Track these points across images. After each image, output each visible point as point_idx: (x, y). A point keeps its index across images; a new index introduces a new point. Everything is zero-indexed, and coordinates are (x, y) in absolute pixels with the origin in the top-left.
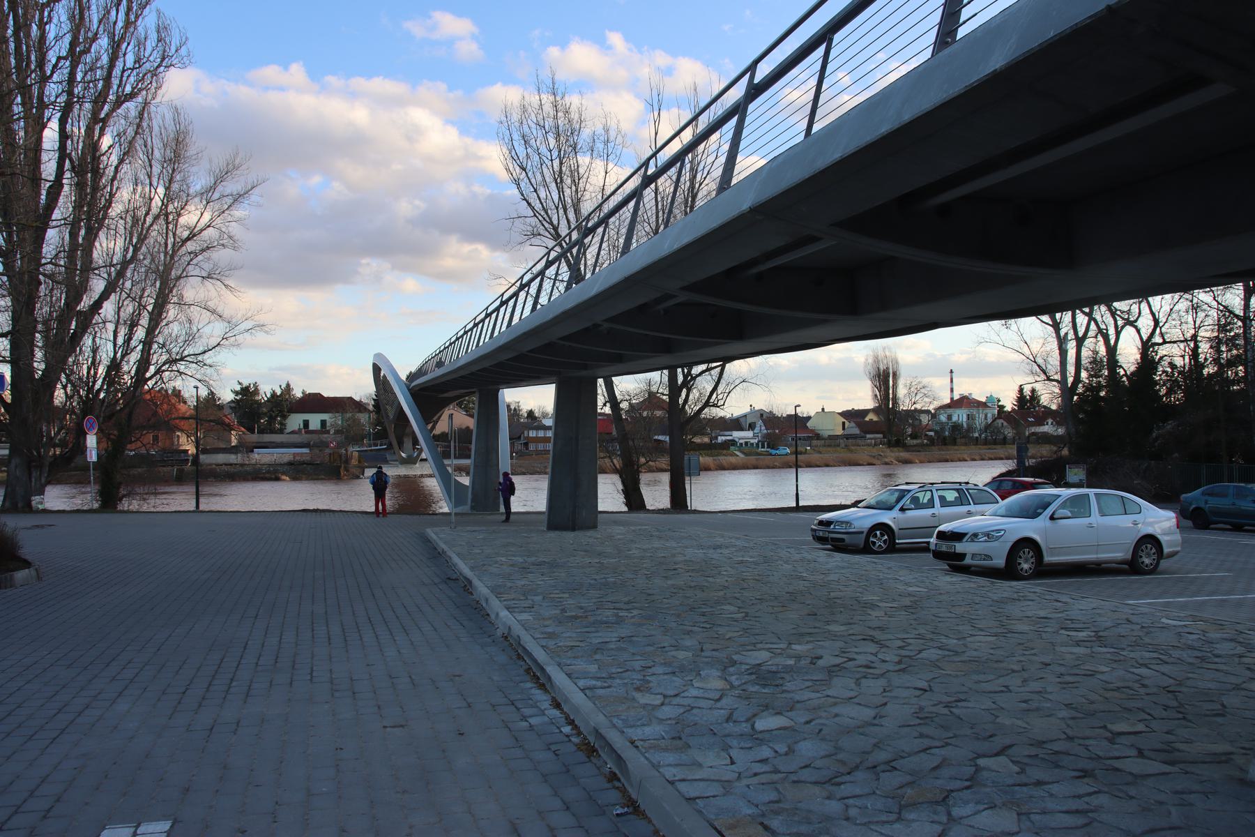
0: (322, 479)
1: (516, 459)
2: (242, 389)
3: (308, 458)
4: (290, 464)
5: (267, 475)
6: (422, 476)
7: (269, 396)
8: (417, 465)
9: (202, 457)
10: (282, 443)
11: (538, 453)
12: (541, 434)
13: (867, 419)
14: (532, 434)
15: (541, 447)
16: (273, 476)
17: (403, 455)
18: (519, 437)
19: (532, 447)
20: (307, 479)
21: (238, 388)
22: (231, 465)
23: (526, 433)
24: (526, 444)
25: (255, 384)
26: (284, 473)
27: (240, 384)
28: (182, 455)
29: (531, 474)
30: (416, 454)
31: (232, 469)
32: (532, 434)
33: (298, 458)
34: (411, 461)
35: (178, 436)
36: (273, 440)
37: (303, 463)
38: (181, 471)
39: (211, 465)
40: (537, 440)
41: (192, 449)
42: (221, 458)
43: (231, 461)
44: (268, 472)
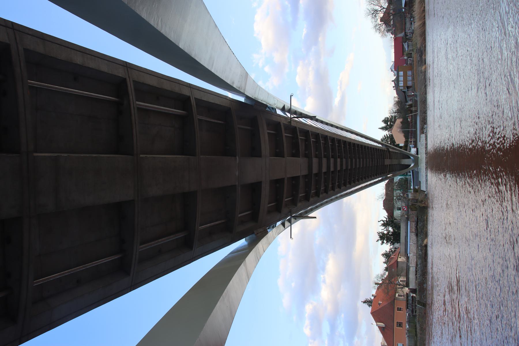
0: (427, 218)
1: (417, 92)
2: (381, 240)
3: (414, 224)
4: (417, 235)
5: (423, 251)
6: (426, 153)
7: (383, 228)
8: (419, 156)
9: (411, 287)
10: (405, 232)
11: (413, 79)
12: (401, 79)
14: (401, 84)
16: (424, 248)
17: (412, 165)
18: (404, 92)
19: (410, 84)
21: (380, 242)
22: (416, 271)
23: (402, 88)
24: (408, 87)
25: (379, 233)
26: (423, 241)
27: (378, 241)
29: (426, 82)
30: (412, 157)
31: (419, 272)
32: (401, 84)
33: (413, 230)
34: (416, 161)
37: (417, 227)
38: (419, 303)
39: (416, 283)
40: (405, 81)
42: (412, 276)
44: (421, 250)
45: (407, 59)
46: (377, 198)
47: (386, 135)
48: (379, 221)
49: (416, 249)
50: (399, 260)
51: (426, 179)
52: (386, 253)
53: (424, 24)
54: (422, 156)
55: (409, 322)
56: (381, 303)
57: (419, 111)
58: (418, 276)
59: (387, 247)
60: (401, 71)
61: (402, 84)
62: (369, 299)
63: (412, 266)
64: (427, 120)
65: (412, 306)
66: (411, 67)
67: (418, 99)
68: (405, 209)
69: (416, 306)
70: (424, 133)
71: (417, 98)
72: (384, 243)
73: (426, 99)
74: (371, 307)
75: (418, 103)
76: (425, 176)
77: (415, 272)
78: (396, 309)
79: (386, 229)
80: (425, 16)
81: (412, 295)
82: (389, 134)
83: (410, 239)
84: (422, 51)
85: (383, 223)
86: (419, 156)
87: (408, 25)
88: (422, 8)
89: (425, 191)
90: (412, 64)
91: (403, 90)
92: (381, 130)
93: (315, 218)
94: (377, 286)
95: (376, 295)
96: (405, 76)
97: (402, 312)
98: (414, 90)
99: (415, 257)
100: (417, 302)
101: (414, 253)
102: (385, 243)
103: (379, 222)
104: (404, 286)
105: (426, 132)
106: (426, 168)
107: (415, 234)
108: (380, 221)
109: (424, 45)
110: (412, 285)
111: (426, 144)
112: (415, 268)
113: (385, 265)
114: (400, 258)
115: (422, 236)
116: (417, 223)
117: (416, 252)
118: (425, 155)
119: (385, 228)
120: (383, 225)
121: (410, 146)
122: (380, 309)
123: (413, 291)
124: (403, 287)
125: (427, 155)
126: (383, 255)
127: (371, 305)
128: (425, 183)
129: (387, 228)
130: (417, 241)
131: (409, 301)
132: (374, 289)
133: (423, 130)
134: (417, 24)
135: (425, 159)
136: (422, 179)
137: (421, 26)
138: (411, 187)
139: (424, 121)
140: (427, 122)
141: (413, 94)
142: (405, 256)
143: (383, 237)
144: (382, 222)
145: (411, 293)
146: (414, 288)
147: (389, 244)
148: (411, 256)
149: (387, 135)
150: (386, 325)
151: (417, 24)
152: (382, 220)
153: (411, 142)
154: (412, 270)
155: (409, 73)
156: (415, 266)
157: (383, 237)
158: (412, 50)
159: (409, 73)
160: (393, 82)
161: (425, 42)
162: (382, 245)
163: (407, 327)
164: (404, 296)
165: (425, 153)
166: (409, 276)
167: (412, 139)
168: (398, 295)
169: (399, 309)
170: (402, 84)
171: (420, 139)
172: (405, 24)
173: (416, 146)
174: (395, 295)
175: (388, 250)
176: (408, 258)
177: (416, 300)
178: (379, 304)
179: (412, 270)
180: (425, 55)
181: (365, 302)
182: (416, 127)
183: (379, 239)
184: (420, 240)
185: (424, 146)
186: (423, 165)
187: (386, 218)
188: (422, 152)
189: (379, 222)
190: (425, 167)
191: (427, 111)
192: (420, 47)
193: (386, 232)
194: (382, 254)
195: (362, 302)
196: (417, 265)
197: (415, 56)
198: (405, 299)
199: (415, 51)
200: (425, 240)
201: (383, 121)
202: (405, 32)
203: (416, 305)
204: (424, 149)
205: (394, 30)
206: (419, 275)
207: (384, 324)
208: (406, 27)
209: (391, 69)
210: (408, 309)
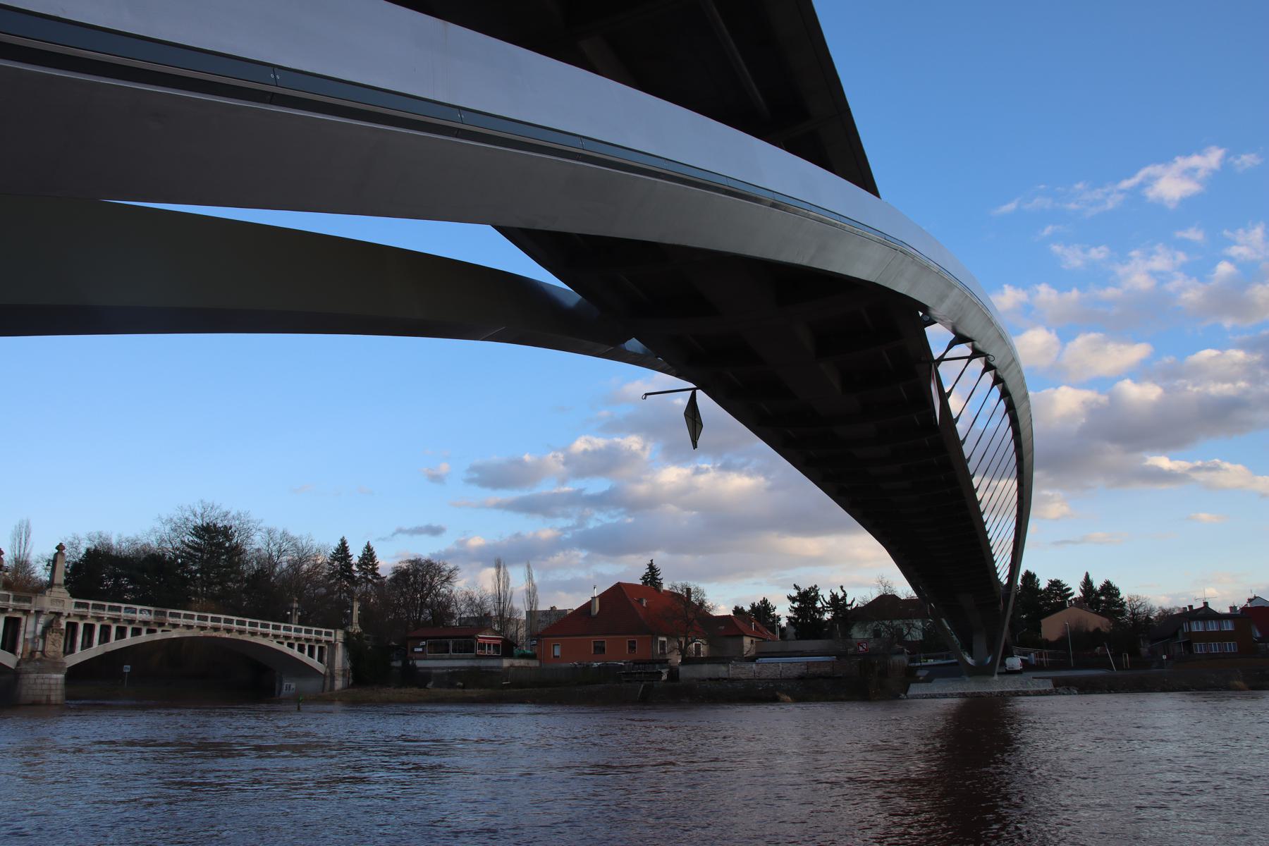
0: (842, 700)
3: (828, 669)
4: (801, 678)
7: (828, 599)
8: (996, 677)
12: (1213, 627)
14: (1197, 627)
17: (969, 660)
18: (1175, 635)
19: (1199, 648)
21: (794, 593)
22: (718, 679)
23: (1185, 626)
24: (1188, 645)
25: (814, 589)
26: (788, 692)
27: (796, 587)
28: (657, 666)
30: (989, 660)
33: (813, 670)
34: (982, 671)
40: (1206, 637)
41: (676, 659)
42: (706, 670)
43: (721, 675)
46: (885, 581)
47: (1070, 592)
48: (844, 589)
49: (769, 677)
50: (747, 641)
51: (938, 696)
52: (770, 609)
54: (996, 685)
55: (605, 669)
56: (643, 604)
57: (1120, 673)
59: (783, 611)
60: (1235, 625)
61: (1198, 628)
62: (659, 577)
63: (728, 671)
64: (1090, 693)
65: (640, 673)
68: (861, 649)
70: (1055, 686)
71: (1157, 668)
72: (793, 603)
74: (640, 583)
76: (944, 692)
77: (717, 677)
78: (632, 638)
79: (825, 605)
83: (791, 663)
85: (840, 598)
86: (996, 677)
89: (906, 693)
91: (1180, 631)
92: (1082, 579)
95: (662, 591)
96: (1221, 636)
97: (627, 652)
99: (751, 675)
100: (649, 683)
101: (759, 673)
102: (792, 605)
103: (842, 587)
105: (1057, 693)
106: (963, 695)
107: (803, 673)
108: (844, 591)
110: (686, 672)
111: (1026, 694)
112: (724, 677)
113: (747, 608)
114: (752, 641)
115: (798, 689)
117: (761, 677)
118: (997, 690)
119: (827, 603)
120: (834, 597)
121: (1032, 654)
123: (674, 674)
125: (997, 696)
127: (645, 583)
128: (927, 693)
129: (827, 607)
130: (788, 679)
132: (670, 587)
133: (1063, 686)
135: (988, 691)
136: (936, 687)
138: (932, 660)
139: (1087, 687)
140: (1085, 694)
142: (756, 653)
143: (806, 599)
144: (840, 595)
145: (667, 670)
146: (680, 676)
147: (791, 615)
148: (752, 667)
149: (1072, 594)
150: (595, 617)
152: (845, 595)
153: (1041, 656)
154: (722, 670)
155: (1231, 647)
156: (731, 676)
157: (806, 599)
160: (1202, 605)
162: (788, 597)
163: (595, 665)
164: (664, 653)
165: (1002, 692)
166: (706, 665)
167: (1046, 657)
168: (664, 642)
169: (632, 647)
170: (1198, 628)
171: (1040, 678)
173: (1027, 666)
174: (663, 636)
175: (777, 612)
176: (752, 659)
177: (653, 681)
178: (640, 601)
179: (722, 670)
181: (651, 567)
182: (1077, 667)
183: (802, 591)
184: (789, 686)
185: (1021, 689)
186: (972, 686)
187: (853, 601)
188: (1006, 684)
189: (842, 587)
190: (966, 691)
191: (1115, 693)
193: (819, 605)
194: (767, 600)
195: (652, 561)
196: (732, 680)
198: (655, 657)
200: (789, 698)
201: (1108, 583)
203: (643, 681)
204: (1013, 690)
206: (709, 686)
207: (599, 613)
209: (1255, 597)
210: (632, 664)
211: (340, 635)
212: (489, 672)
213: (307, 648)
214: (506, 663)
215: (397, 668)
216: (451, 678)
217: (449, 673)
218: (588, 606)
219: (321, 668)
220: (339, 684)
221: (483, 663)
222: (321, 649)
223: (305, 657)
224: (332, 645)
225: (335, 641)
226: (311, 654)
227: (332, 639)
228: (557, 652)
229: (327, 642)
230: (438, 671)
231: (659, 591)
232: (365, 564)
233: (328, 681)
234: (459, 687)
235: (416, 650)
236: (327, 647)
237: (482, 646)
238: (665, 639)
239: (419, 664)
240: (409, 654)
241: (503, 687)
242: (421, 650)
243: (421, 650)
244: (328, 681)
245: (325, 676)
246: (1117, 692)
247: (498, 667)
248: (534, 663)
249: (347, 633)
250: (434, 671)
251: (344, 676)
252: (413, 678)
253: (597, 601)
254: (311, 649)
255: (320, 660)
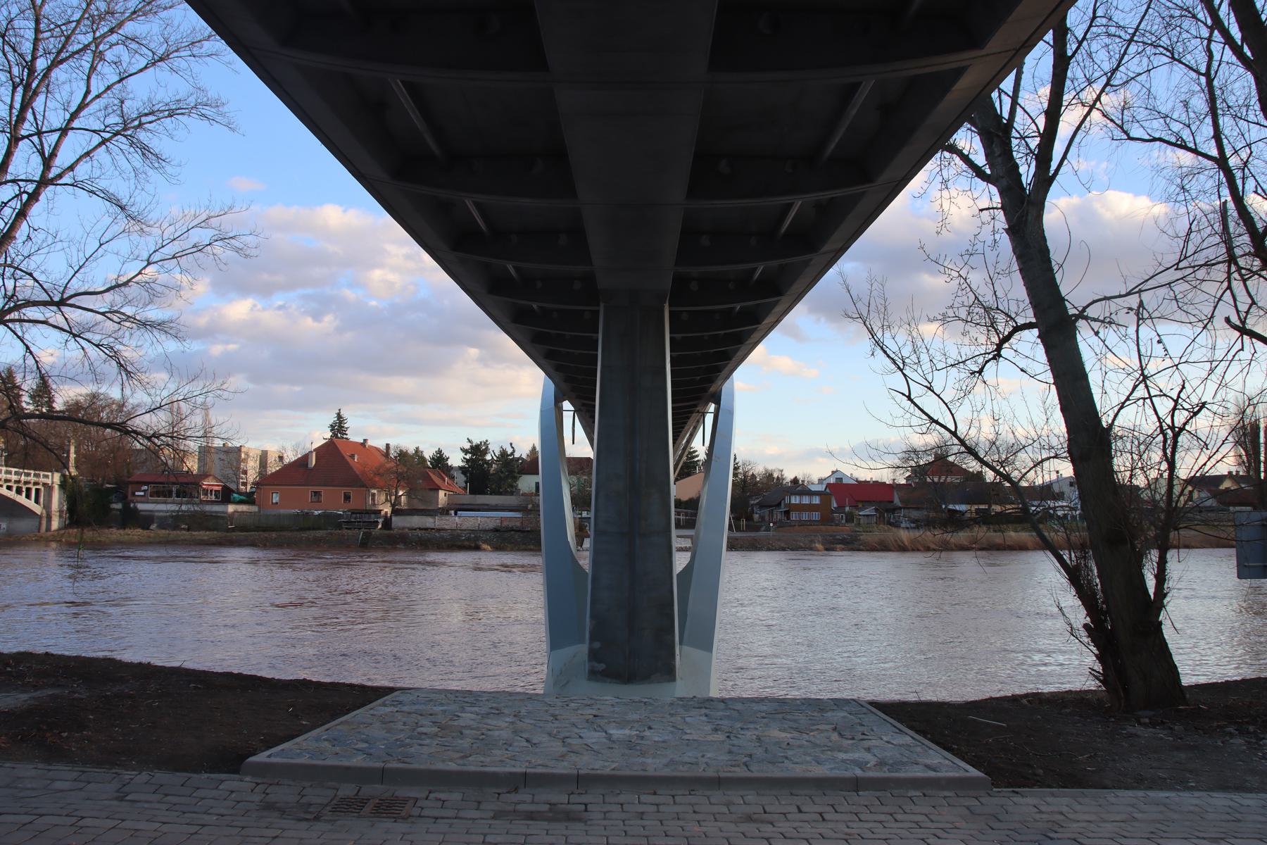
0: (531, 550)
1: (775, 530)
3: (518, 524)
4: (496, 530)
5: (466, 543)
9: (394, 519)
10: (497, 505)
11: (802, 523)
12: (806, 500)
13: (1223, 487)
14: (795, 500)
15: (805, 516)
16: (473, 545)
18: (779, 504)
19: (794, 516)
20: (512, 550)
21: (467, 446)
22: (426, 529)
23: (787, 501)
24: (787, 513)
25: (486, 443)
26: (485, 542)
27: (469, 441)
28: (373, 516)
29: (792, 550)
31: (426, 535)
32: (795, 500)
33: (505, 524)
35: (374, 495)
36: (487, 503)
38: (367, 536)
39: (404, 528)
40: (801, 508)
42: (416, 521)
44: (468, 539)
45: (844, 512)
47: (697, 453)
50: (441, 494)
53: (902, 548)
55: (325, 516)
58: (419, 533)
59: (456, 459)
60: (821, 500)
62: (346, 426)
66: (827, 519)
67: (762, 533)
69: (360, 529)
73: (759, 550)
75: (753, 534)
77: (424, 527)
80: (918, 550)
81: (381, 521)
82: (698, 461)
84: (852, 544)
87: (915, 514)
88: (933, 546)
90: (832, 522)
93: (573, 443)
94: (383, 447)
96: (811, 508)
98: (780, 525)
99: (454, 526)
103: (511, 444)
104: (393, 506)
109: (861, 547)
110: (397, 522)
116: (519, 531)
117: (463, 528)
122: (343, 457)
123: (387, 523)
124: (391, 501)
126: (440, 452)
130: (485, 531)
131: (367, 515)
134: (904, 535)
137: (900, 544)
141: (771, 525)
144: (509, 451)
146: (393, 526)
149: (697, 456)
150: (312, 470)
151: (904, 535)
152: (514, 451)
154: (429, 522)
155: (816, 516)
156: (437, 527)
158: (859, 524)
159: (816, 516)
161: (867, 550)
163: (316, 513)
164: (374, 504)
169: (347, 498)
172: (917, 509)
176: (445, 512)
178: (352, 456)
179: (429, 522)
180: (843, 550)
181: (339, 416)
183: (474, 444)
189: (511, 444)
192: (860, 540)
193: (488, 457)
196: (439, 530)
197: (845, 530)
199: (857, 529)
202: (900, 508)
205: (911, 485)
208: (911, 510)
209: (837, 471)
211: (57, 477)
212: (215, 517)
213: (24, 490)
214: (231, 508)
215: (117, 510)
216: (174, 521)
217: (172, 517)
218: (304, 459)
219: (38, 509)
220: (55, 524)
221: (208, 508)
222: (38, 491)
223: (22, 499)
224: (49, 488)
225: (53, 483)
226: (28, 496)
227: (49, 481)
228: (276, 498)
229: (45, 485)
230: (161, 514)
231: (365, 446)
232: (39, 396)
233: (44, 522)
234: (184, 529)
235: (137, 493)
236: (43, 489)
237: (206, 492)
238: (375, 491)
239: (141, 506)
240: (130, 498)
241: (228, 530)
242: (142, 493)
243: (142, 493)
244: (44, 522)
245: (40, 517)
246: (736, 550)
247: (223, 512)
248: (254, 509)
249: (64, 476)
250: (156, 514)
251: (60, 516)
252: (131, 518)
253: (314, 454)
254: (29, 490)
255: (37, 501)
